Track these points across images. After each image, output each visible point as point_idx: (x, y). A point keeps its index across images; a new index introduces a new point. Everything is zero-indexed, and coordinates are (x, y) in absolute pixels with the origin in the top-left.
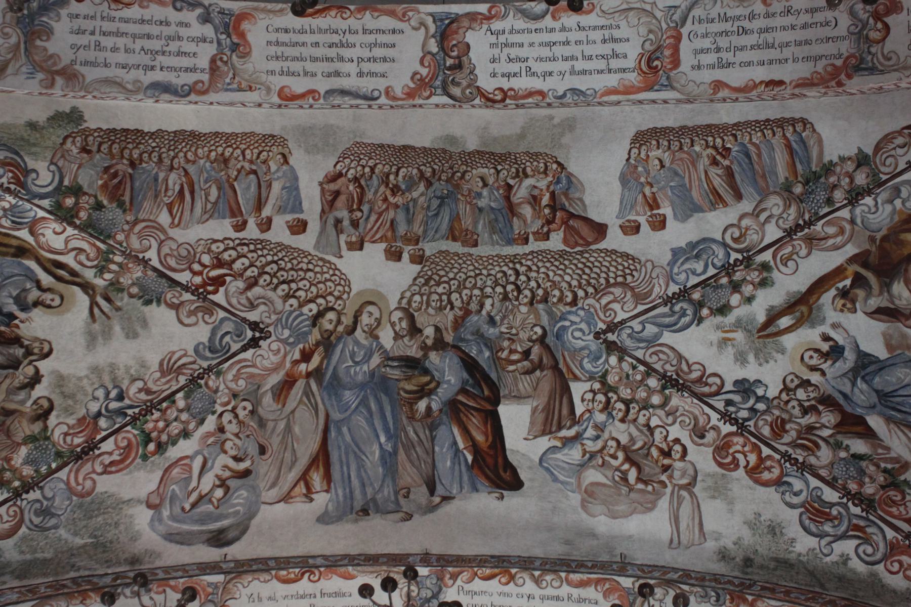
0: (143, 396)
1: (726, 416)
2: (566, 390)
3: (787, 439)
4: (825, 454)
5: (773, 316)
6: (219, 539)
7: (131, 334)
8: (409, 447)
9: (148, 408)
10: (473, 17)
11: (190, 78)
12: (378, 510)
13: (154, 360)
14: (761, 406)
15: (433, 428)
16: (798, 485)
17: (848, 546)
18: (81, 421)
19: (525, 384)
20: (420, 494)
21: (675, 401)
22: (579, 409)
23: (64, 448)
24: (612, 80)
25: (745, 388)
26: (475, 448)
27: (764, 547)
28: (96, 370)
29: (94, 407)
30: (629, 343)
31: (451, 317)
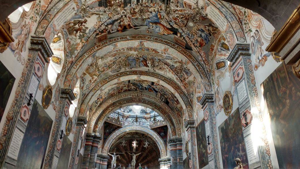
1: (170, 68)
4: (179, 74)
5: (176, 62)
6: (118, 72)
7: (106, 59)
8: (137, 64)
9: (109, 65)
10: (144, 41)
11: (111, 50)
13: (109, 61)
15: (140, 62)
16: (176, 76)
17: (179, 83)
21: (165, 65)
23: (101, 71)
24: (161, 49)
25: (173, 65)
27: (172, 78)
28: (103, 63)
29: (103, 66)
30: (161, 59)
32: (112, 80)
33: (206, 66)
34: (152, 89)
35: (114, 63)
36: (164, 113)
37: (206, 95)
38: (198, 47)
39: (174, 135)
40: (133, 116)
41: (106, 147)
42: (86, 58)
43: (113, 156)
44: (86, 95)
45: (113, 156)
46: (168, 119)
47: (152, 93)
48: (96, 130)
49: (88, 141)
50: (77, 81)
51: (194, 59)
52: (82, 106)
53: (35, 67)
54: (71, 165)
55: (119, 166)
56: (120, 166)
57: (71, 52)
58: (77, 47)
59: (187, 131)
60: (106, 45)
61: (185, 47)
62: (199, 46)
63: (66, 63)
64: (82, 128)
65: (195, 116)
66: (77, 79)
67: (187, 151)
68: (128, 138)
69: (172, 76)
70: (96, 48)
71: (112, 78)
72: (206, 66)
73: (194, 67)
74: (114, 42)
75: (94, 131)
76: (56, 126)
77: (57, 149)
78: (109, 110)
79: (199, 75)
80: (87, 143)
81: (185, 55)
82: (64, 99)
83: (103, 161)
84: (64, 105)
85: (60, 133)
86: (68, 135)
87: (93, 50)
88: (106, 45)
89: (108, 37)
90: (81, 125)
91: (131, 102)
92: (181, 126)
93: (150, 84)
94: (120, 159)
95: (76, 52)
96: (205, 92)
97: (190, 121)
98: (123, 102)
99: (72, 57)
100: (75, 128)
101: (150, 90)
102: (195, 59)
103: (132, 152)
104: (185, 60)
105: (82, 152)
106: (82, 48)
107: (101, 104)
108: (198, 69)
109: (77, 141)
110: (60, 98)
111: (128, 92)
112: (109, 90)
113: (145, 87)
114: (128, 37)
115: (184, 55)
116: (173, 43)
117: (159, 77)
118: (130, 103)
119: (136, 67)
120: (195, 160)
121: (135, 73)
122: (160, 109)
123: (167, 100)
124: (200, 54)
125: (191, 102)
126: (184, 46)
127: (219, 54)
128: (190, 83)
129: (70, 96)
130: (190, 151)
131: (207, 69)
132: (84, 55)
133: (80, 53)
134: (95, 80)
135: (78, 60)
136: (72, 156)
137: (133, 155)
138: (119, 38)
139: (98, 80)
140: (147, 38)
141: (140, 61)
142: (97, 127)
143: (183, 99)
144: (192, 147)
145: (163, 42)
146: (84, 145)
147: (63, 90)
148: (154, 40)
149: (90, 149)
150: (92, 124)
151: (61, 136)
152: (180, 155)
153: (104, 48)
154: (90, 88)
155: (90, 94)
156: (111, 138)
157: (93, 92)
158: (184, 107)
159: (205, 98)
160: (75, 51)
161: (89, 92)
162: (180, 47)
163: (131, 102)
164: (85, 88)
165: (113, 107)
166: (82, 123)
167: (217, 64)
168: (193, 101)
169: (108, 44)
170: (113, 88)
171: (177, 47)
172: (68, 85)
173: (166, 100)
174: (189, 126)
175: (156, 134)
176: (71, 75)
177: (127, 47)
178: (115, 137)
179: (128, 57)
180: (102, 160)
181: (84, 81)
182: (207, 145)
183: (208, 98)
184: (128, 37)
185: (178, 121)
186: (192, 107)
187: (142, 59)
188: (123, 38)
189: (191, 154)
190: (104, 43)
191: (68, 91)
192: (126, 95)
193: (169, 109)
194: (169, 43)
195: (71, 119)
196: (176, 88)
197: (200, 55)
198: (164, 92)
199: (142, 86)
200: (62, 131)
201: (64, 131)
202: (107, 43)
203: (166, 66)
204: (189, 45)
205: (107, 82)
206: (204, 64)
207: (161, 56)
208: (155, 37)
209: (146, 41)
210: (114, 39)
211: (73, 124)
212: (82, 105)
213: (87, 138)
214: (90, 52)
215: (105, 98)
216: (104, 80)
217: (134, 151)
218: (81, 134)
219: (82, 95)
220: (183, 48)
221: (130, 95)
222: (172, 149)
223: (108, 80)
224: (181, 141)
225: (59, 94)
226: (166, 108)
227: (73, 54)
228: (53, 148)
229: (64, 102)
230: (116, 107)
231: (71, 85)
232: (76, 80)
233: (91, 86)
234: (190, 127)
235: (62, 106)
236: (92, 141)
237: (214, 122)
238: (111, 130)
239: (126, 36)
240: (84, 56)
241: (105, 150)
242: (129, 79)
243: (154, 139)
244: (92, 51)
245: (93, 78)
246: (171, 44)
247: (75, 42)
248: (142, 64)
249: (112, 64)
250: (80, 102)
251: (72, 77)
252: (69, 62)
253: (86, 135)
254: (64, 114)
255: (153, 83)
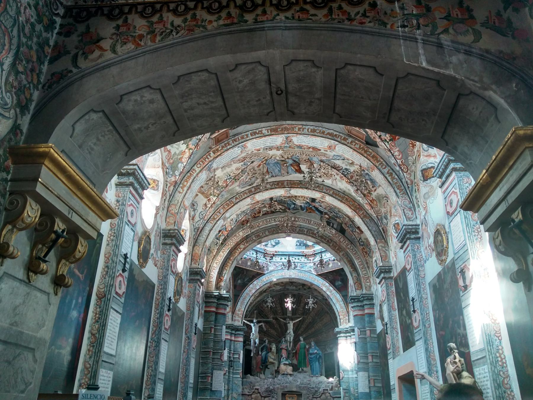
0: (234, 175)
1: (342, 174)
2: (313, 164)
3: (353, 179)
6: (250, 185)
8: (283, 169)
9: (235, 176)
12: (278, 176)
13: (234, 169)
14: (349, 173)
17: (361, 199)
18: (224, 181)
19: (305, 163)
20: (287, 174)
21: (333, 170)
22: (315, 167)
25: (346, 169)
26: (296, 169)
27: (347, 191)
28: (224, 174)
29: (226, 179)
30: (325, 161)
31: (290, 156)
32: (241, 200)
33: (405, 174)
34: (313, 208)
35: (243, 172)
36: (338, 249)
37: (407, 227)
38: (388, 142)
39: (358, 289)
40: (282, 252)
41: (239, 311)
42: (197, 174)
43: (252, 325)
44: (199, 230)
45: (252, 325)
46: (345, 260)
47: (313, 214)
48: (220, 286)
49: (209, 304)
50: (185, 213)
51: (382, 163)
52: (195, 249)
53: (127, 212)
54: (186, 350)
55: (265, 342)
56: (267, 341)
57: (173, 165)
58: (182, 158)
59: (379, 283)
60: (228, 147)
61: (365, 142)
62: (390, 140)
63: (167, 185)
64: (198, 287)
65: (393, 258)
66: (185, 210)
67: (382, 319)
68: (277, 291)
69: (346, 188)
70: (212, 154)
71: (242, 196)
72: (405, 174)
73: (382, 176)
74: (240, 141)
75: (218, 287)
76: (160, 292)
77: (165, 329)
78: (239, 250)
79: (392, 190)
80: (208, 309)
81: (366, 155)
82: (168, 247)
83: (235, 335)
84: (169, 256)
85: (167, 302)
86: (177, 301)
87: (207, 160)
88: (228, 147)
89: (231, 135)
90: (197, 283)
91: (276, 233)
92: (371, 272)
93: (308, 201)
94: (265, 329)
95: (181, 166)
96: (404, 221)
97: (383, 268)
98: (263, 234)
99: (175, 174)
100: (187, 288)
101: (310, 211)
102: (384, 162)
103: (286, 316)
104: (366, 164)
105: (200, 326)
106: (190, 158)
107: (225, 240)
108: (390, 180)
109: (192, 309)
110: (162, 245)
111: (272, 214)
112: (237, 215)
113: (301, 206)
114: (264, 131)
115: (364, 156)
116: (343, 136)
117: (324, 190)
118: (276, 235)
119: (282, 175)
120: (395, 335)
121: (280, 185)
122: (330, 243)
123: (342, 227)
124: (391, 153)
125: (384, 232)
126: (363, 140)
127: (426, 154)
128: (380, 198)
129: (177, 240)
130: (386, 319)
131: (407, 180)
132: (193, 168)
133: (187, 167)
134: (212, 202)
135: (185, 178)
136: (186, 334)
137: (289, 323)
138: (249, 133)
139: (219, 203)
140: (297, 131)
141: (288, 165)
142: (221, 279)
143: (370, 228)
144: (389, 312)
145: (326, 135)
146: (203, 312)
147: (166, 231)
148: (309, 133)
149: (213, 318)
150: (212, 276)
151: (169, 306)
152: (371, 324)
153: (226, 154)
154: (206, 217)
155: (206, 227)
156: (247, 294)
157: (211, 223)
158: (372, 241)
159: (404, 232)
160: (178, 164)
161: (204, 224)
162: (356, 142)
163: (278, 233)
164: (197, 218)
165: (246, 244)
166: (196, 278)
167: (422, 171)
168: (387, 231)
169: (231, 146)
170: (244, 211)
171: (351, 142)
172: (173, 222)
173: (339, 227)
174: (382, 275)
175: (327, 284)
176: (176, 205)
177: (263, 147)
178: (254, 291)
179: (266, 160)
180: (233, 333)
181: (195, 207)
182: (412, 312)
183: (409, 233)
184: (264, 131)
185: (365, 263)
186: (386, 242)
187: (291, 162)
188: (255, 133)
189: (388, 326)
190: (225, 145)
191: (173, 233)
192: (268, 220)
193: (347, 242)
194: (336, 135)
195: (180, 275)
196: (356, 207)
197: (393, 155)
198: (335, 213)
199: (294, 204)
200: (170, 299)
201: (172, 299)
202: (229, 145)
203: (334, 172)
204: (372, 138)
205: (233, 204)
206: (400, 171)
207: (325, 155)
208: (312, 127)
209: (295, 135)
210: (240, 136)
211: (183, 281)
212: (196, 247)
213: (207, 300)
214: (203, 162)
215: (232, 229)
216: (228, 202)
217: (289, 314)
218: (197, 297)
219: (193, 230)
220: (362, 142)
221: (275, 220)
222: (356, 314)
223: (234, 200)
224: (372, 299)
225: (160, 239)
226: (342, 240)
227: (175, 170)
228: (159, 328)
229: (169, 251)
230: (252, 243)
231: (177, 221)
232: (183, 212)
233: (208, 213)
234: (383, 278)
235: (166, 258)
236: (215, 305)
237: (422, 274)
238: (245, 280)
239: (260, 130)
240: (194, 170)
241: (238, 315)
242: (271, 196)
243: (324, 293)
244: (206, 161)
245: (209, 200)
246: (340, 137)
247: (178, 149)
248: (291, 169)
249: (240, 173)
250: (191, 243)
251: (177, 208)
252: (171, 184)
253: (204, 295)
254: (170, 272)
255: (313, 200)
